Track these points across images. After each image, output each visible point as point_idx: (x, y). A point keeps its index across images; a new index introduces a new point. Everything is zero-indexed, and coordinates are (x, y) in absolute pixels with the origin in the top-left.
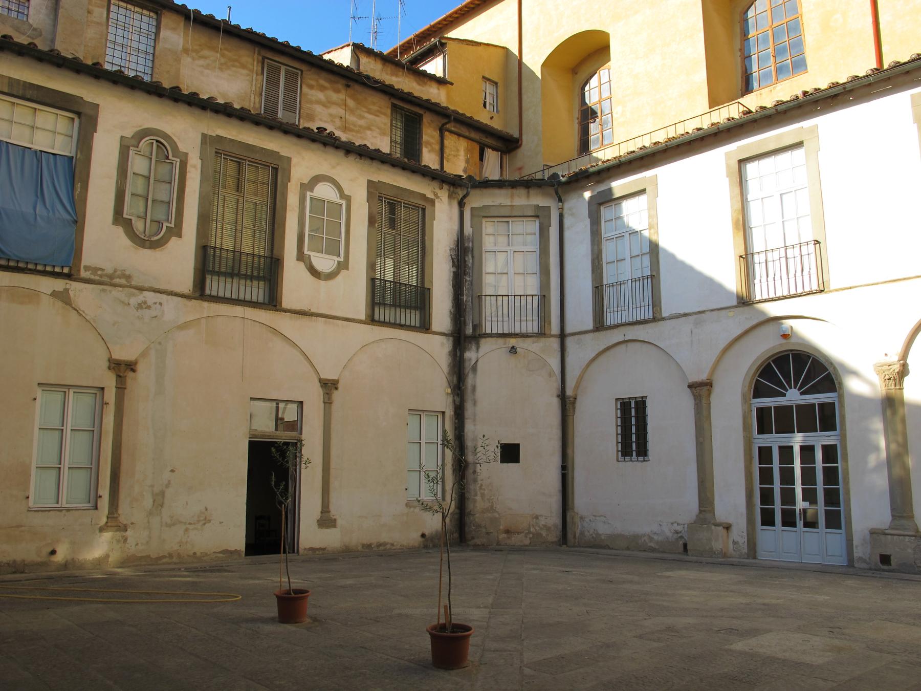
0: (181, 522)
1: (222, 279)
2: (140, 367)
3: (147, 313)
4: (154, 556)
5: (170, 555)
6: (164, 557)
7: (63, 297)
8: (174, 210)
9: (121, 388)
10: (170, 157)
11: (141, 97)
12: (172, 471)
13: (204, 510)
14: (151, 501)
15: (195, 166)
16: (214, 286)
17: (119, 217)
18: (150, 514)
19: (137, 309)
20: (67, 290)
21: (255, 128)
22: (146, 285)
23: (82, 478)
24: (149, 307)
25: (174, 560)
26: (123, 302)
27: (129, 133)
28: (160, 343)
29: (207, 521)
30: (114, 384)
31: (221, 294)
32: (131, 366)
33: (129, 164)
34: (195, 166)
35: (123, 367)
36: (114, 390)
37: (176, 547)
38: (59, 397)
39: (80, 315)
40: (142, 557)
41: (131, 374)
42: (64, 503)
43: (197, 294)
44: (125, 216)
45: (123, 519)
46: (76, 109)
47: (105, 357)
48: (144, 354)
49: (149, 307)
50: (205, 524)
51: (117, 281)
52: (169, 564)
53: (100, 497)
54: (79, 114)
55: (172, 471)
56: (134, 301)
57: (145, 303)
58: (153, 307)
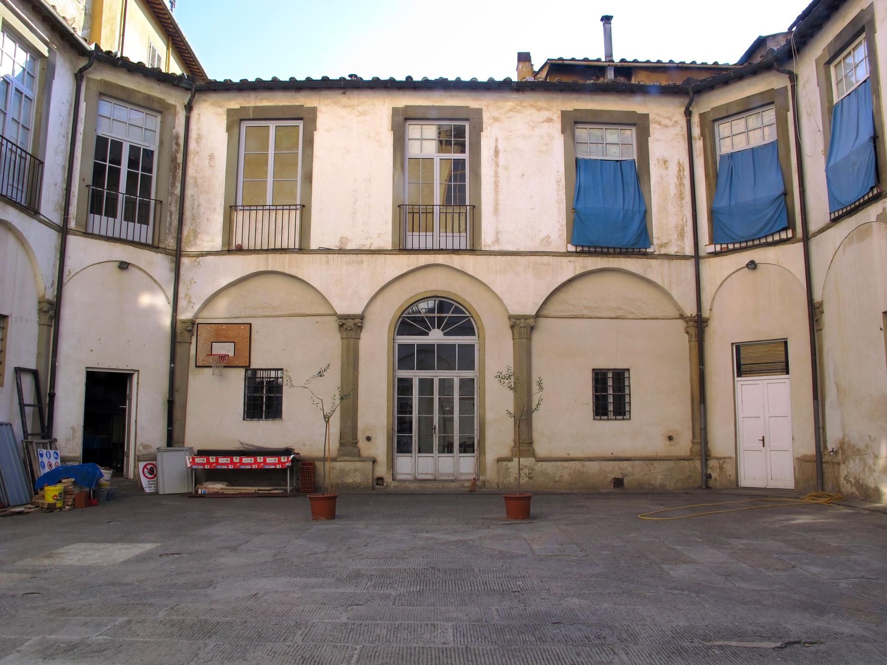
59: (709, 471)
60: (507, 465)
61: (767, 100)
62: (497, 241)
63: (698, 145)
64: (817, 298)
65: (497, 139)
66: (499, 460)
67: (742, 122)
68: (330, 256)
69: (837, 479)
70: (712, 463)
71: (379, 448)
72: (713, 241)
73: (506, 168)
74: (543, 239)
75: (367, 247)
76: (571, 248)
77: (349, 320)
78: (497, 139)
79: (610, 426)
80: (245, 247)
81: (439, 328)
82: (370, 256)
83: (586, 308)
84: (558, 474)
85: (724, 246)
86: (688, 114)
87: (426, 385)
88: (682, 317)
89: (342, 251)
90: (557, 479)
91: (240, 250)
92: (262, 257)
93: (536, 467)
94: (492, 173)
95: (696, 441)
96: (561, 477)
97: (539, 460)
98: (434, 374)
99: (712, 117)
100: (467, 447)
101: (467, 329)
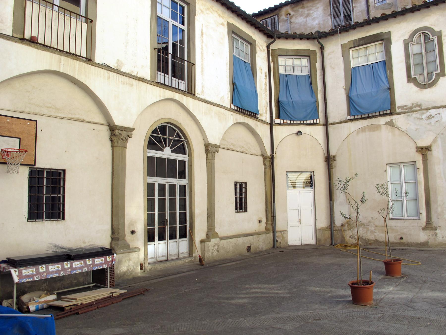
2: (433, 148)
3: (433, 121)
7: (391, 124)
8: (438, 63)
9: (425, 160)
10: (431, 37)
11: (409, 16)
17: (410, 78)
19: (427, 120)
20: (392, 120)
22: (430, 107)
23: (411, 205)
24: (433, 117)
26: (419, 119)
27: (407, 37)
28: (442, 134)
30: (421, 159)
32: (428, 148)
33: (410, 51)
35: (424, 150)
36: (421, 162)
38: (397, 169)
39: (400, 130)
41: (429, 152)
44: (412, 77)
45: (434, 224)
46: (381, 39)
47: (415, 146)
48: (435, 141)
49: (433, 117)
51: (414, 109)
53: (421, 213)
54: (383, 40)
56: (424, 116)
57: (431, 115)
58: (435, 116)
59: (277, 239)
60: (208, 244)
61: (309, 55)
62: (203, 92)
63: (272, 65)
65: (202, 25)
66: (202, 241)
67: (291, 60)
68: (111, 73)
69: (343, 237)
70: (278, 234)
71: (139, 240)
75: (135, 74)
76: (233, 107)
77: (124, 132)
78: (202, 25)
79: (242, 215)
80: (41, 41)
81: (169, 146)
82: (137, 81)
83: (232, 144)
85: (285, 121)
86: (268, 47)
87: (162, 187)
88: (263, 156)
89: (118, 72)
91: (33, 41)
92: (55, 57)
93: (221, 245)
96: (229, 249)
98: (166, 181)
99: (278, 53)
100: (183, 235)
101: (181, 150)
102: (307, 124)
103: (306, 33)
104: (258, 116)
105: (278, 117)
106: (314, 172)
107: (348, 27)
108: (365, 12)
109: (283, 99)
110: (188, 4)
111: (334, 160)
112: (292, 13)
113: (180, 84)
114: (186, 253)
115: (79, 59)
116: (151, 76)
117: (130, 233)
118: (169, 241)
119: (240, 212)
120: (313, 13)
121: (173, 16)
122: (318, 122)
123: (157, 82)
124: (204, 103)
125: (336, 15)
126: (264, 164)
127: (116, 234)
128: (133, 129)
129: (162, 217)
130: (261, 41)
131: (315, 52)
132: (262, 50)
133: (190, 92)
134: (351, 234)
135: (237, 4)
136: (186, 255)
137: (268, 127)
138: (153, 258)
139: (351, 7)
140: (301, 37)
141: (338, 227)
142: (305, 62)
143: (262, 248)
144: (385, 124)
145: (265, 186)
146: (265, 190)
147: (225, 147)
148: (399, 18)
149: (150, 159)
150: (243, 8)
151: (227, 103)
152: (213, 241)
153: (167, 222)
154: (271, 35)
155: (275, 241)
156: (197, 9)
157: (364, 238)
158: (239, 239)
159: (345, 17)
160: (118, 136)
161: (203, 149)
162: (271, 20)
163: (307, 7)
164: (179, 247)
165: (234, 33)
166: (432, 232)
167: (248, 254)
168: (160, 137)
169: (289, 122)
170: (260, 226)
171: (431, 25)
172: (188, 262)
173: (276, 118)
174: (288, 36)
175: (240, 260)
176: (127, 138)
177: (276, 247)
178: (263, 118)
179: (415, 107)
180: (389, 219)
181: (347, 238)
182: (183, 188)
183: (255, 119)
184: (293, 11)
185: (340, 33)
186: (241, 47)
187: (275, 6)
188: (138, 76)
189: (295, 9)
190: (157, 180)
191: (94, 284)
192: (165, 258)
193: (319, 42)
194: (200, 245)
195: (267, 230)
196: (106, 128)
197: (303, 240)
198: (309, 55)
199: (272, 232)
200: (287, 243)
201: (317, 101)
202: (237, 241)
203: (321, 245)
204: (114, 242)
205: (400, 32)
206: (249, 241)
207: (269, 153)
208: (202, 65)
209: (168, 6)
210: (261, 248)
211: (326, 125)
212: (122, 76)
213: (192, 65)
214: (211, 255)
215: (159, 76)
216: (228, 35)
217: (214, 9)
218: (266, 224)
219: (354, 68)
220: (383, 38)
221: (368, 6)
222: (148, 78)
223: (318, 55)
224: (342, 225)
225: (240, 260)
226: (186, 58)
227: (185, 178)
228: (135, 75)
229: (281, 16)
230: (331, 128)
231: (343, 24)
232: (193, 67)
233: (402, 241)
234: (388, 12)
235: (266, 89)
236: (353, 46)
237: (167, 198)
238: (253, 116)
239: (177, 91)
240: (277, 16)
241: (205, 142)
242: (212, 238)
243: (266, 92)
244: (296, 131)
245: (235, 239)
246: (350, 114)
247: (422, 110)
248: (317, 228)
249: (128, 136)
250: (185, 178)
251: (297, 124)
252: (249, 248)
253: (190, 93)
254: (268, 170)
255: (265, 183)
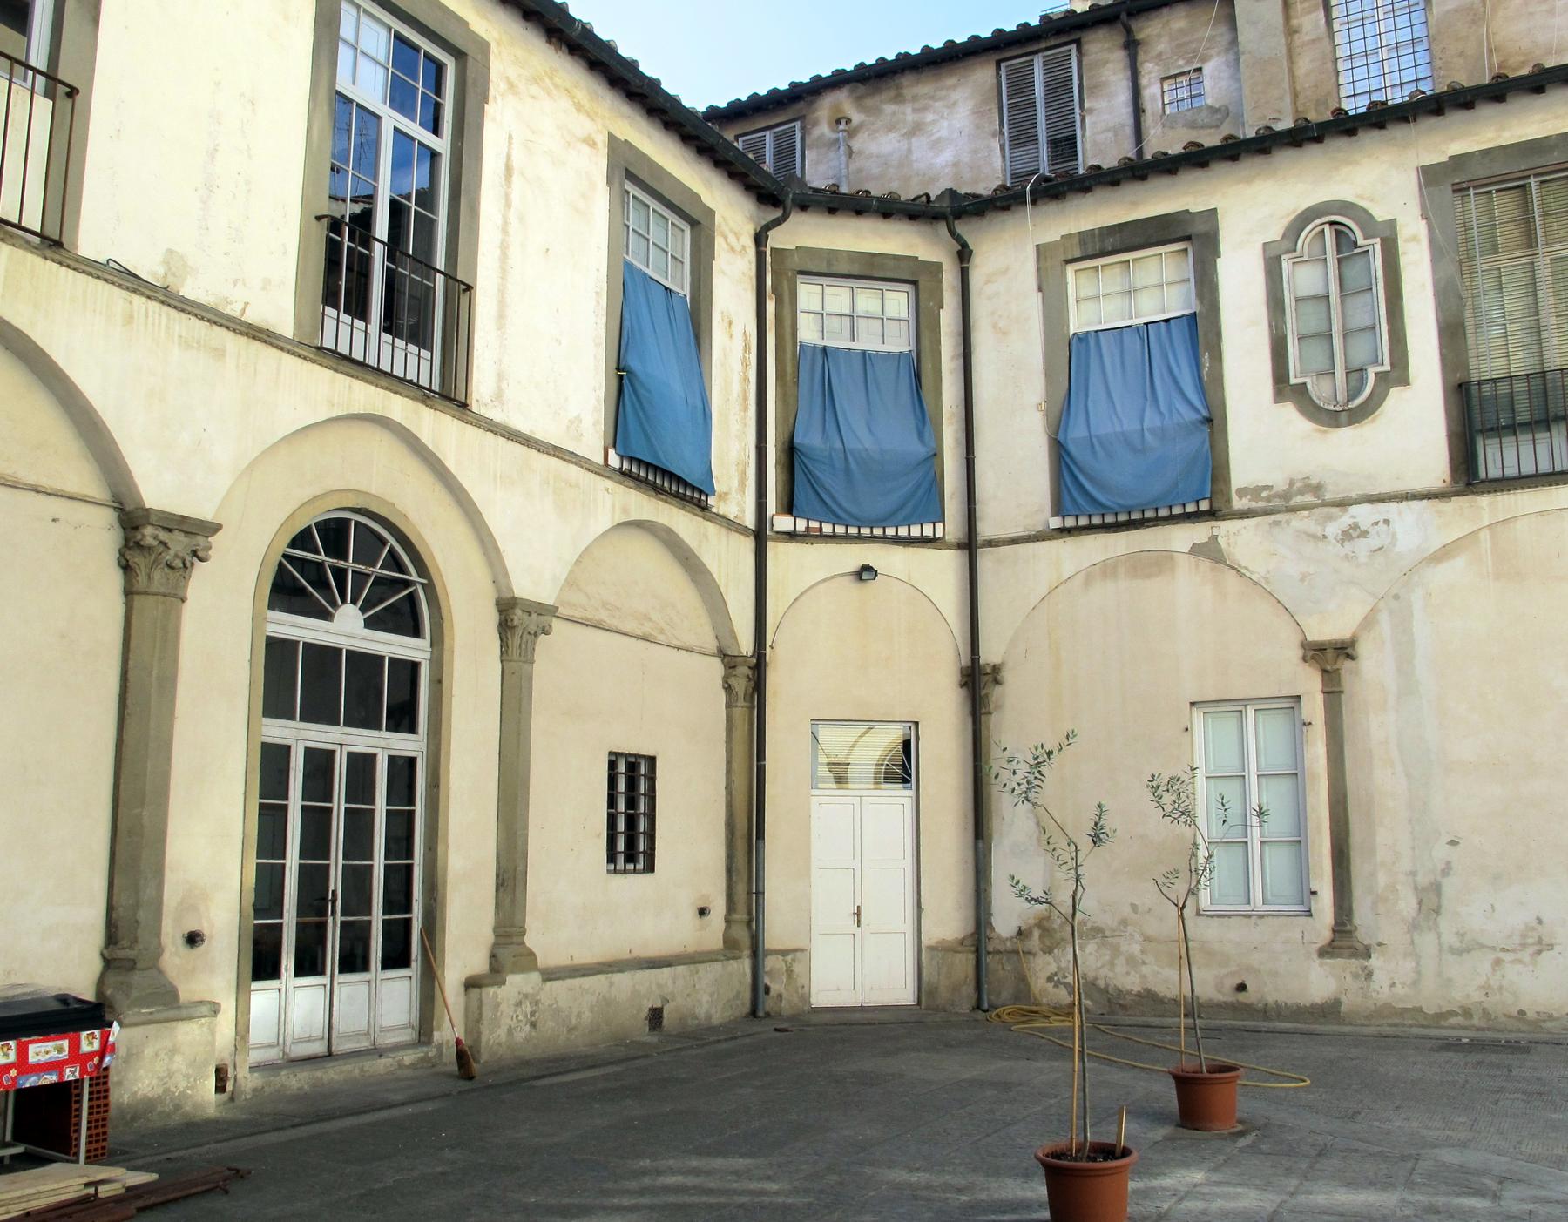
0: (1482, 946)
1: (1525, 438)
2: (1364, 649)
3: (1362, 547)
4: (1430, 1009)
5: (1467, 1013)
6: (1452, 1013)
7: (1209, 552)
8: (1385, 337)
9: (1333, 693)
10: (1360, 242)
11: (1285, 158)
12: (1453, 843)
13: (1534, 923)
14: (1414, 903)
15: (1414, 239)
16: (1495, 457)
17: (1283, 386)
18: (1414, 927)
19: (1342, 542)
21: (1539, 101)
22: (1353, 494)
25: (1476, 1021)
26: (1314, 536)
27: (1275, 233)
28: (1396, 597)
29: (1543, 946)
31: (1511, 471)
32: (1345, 650)
33: (1285, 285)
34: (1414, 239)
35: (1330, 654)
36: (1320, 698)
37: (1477, 996)
38: (1230, 723)
39: (1242, 575)
40: (1406, 1010)
41: (1348, 664)
42: (1258, 904)
43: (1461, 486)
44: (1293, 381)
45: (1363, 935)
46: (1180, 234)
47: (1295, 640)
48: (1369, 622)
49: (1364, 534)
50: (1539, 952)
51: (1298, 500)
52: (1465, 1028)
53: (1314, 893)
54: (1188, 238)
55: (1453, 843)
56: (1333, 529)
57: (1355, 527)
58: (1373, 531)
59: (767, 981)
61: (914, 276)
62: (499, 396)
64: (990, 654)
65: (510, 137)
66: (472, 984)
68: (138, 301)
69: (1022, 979)
70: (771, 963)
72: (789, 507)
73: (521, 219)
74: (572, 422)
75: (233, 310)
76: (614, 461)
78: (510, 137)
79: (633, 885)
81: (354, 602)
82: (244, 340)
83: (605, 605)
84: (575, 1011)
85: (814, 524)
86: (760, 239)
87: (320, 762)
88: (722, 654)
89: (167, 297)
90: (574, 1021)
93: (543, 997)
94: (500, 222)
95: (736, 917)
96: (579, 1015)
97: (550, 975)
98: (338, 738)
99: (796, 262)
100: (396, 957)
101: (405, 619)
102: (897, 540)
103: (907, 195)
104: (711, 501)
105: (789, 507)
106: (917, 724)
107: (1064, 182)
108: (1129, 131)
109: (809, 439)
110: (459, 55)
111: (997, 682)
112: (857, 118)
113: (412, 360)
114: (404, 1027)
115: (12, 236)
116: (298, 324)
117: (180, 941)
118: (339, 978)
119: (625, 871)
120: (934, 122)
121: (400, 97)
122: (939, 534)
123: (320, 349)
124: (501, 440)
125: (1021, 136)
126: (728, 688)
127: (125, 943)
128: (215, 528)
129: (313, 880)
130: (732, 213)
131: (935, 269)
132: (738, 248)
133: (450, 394)
134: (1053, 968)
135: (647, 69)
136: (407, 1036)
137: (747, 546)
138: (270, 1046)
139: (1077, 111)
140: (888, 209)
141: (1004, 941)
142: (898, 301)
143: (709, 1017)
144: (1191, 552)
145: (729, 772)
146: (728, 788)
147: (577, 614)
148: (1249, 165)
149: (278, 652)
150: (669, 87)
151: (591, 439)
152: (517, 983)
153: (334, 901)
154: (774, 194)
155: (758, 988)
156: (493, 76)
157: (1101, 983)
158: (617, 977)
159: (1053, 143)
160: (152, 548)
161: (493, 617)
162: (777, 137)
163: (915, 98)
164: (377, 1003)
165: (631, 176)
166: (1354, 964)
167: (653, 1039)
168: (321, 565)
169: (827, 528)
170: (702, 928)
171: (1362, 197)
172: (413, 1066)
173: (778, 513)
174: (835, 203)
175: (619, 1062)
176: (188, 559)
177: (761, 1014)
178: (729, 509)
179: (1301, 492)
180: (1198, 914)
181: (1039, 983)
182: (403, 769)
183: (698, 511)
184: (861, 108)
185: (1034, 202)
186: (655, 234)
187: (793, 85)
188: (249, 317)
189: (869, 102)
190: (303, 734)
191: (19, 1149)
192: (319, 1048)
193: (952, 233)
194: (462, 999)
195: (730, 944)
196: (108, 516)
197: (867, 989)
198: (914, 276)
199: (747, 952)
200: (806, 998)
201: (936, 455)
202: (611, 984)
203: (936, 1009)
204: (112, 978)
205: (1252, 211)
206: (659, 986)
207: (746, 645)
208: (502, 292)
209: (382, 59)
210: (702, 1016)
211: (970, 545)
212: (183, 315)
213: (461, 290)
214: (503, 1038)
215: (330, 325)
216: (609, 182)
217: (558, 81)
218: (728, 921)
219: (1082, 338)
220: (1190, 231)
221: (1138, 110)
222: (287, 330)
223: (949, 278)
224: (1020, 933)
225: (619, 1062)
226: (440, 262)
227: (412, 729)
228: (236, 314)
229: (816, 123)
230: (986, 559)
231: (1045, 169)
232: (464, 299)
233: (1242, 997)
234: (1211, 140)
235: (745, 399)
236: (1078, 254)
237: (339, 804)
238: (691, 501)
239: (399, 387)
240: (797, 124)
241: (498, 590)
242: (513, 972)
243: (746, 408)
244: (854, 566)
245: (601, 977)
246: (1058, 509)
247: (1325, 504)
248: (925, 941)
249: (194, 553)
250: (412, 729)
251: (859, 538)
252: (656, 1016)
253: (449, 399)
254: (740, 712)
255: (729, 762)
